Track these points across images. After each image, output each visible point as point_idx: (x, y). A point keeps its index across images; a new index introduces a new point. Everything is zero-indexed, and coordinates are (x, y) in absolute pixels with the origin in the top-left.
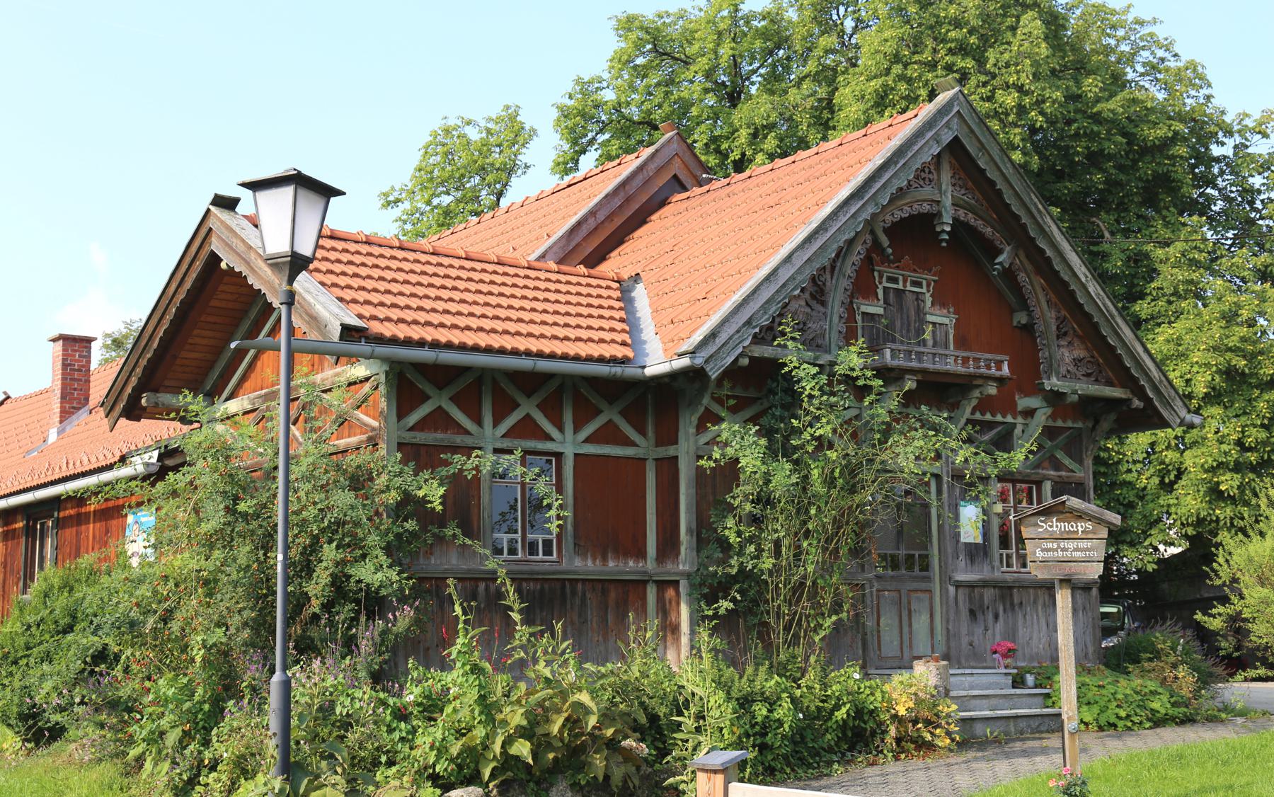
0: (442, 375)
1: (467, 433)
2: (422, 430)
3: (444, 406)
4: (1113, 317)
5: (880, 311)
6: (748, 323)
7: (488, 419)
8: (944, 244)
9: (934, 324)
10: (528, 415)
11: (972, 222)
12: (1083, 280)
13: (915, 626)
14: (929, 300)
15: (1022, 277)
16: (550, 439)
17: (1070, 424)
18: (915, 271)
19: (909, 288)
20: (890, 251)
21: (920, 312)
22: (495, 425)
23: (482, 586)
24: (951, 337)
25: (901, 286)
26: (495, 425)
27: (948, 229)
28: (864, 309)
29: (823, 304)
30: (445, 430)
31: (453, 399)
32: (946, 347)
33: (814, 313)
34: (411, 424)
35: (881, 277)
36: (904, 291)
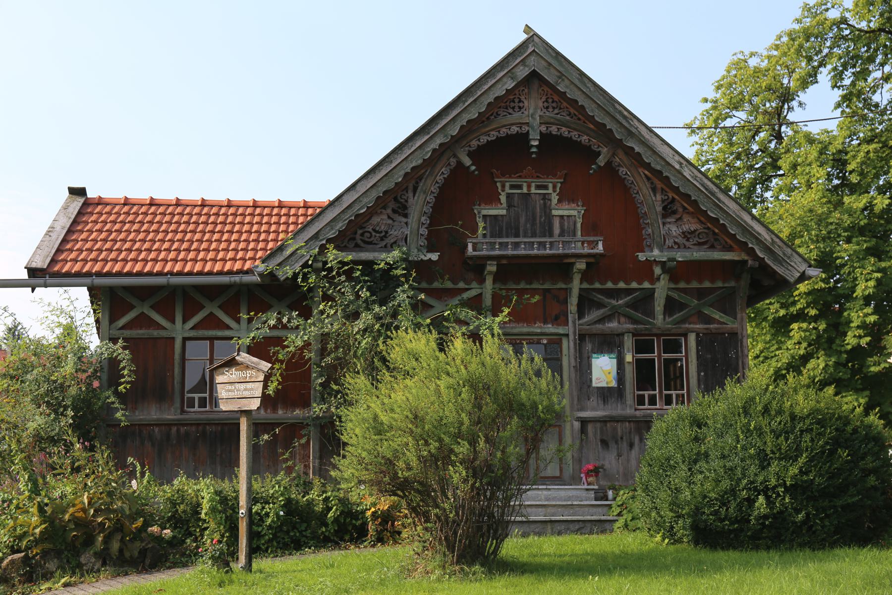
0: (143, 293)
1: (165, 328)
2: (131, 329)
3: (145, 312)
4: (713, 194)
5: (504, 212)
6: (316, 236)
8: (534, 156)
9: (562, 217)
11: (566, 134)
12: (677, 166)
14: (555, 198)
15: (623, 171)
16: (228, 327)
17: (719, 284)
18: (538, 177)
19: (533, 190)
20: (473, 168)
22: (184, 322)
23: (174, 429)
24: (579, 225)
25: (525, 190)
26: (184, 322)
27: (536, 143)
28: (485, 212)
29: (406, 216)
30: (148, 327)
31: (152, 307)
32: (574, 235)
33: (396, 223)
34: (120, 325)
35: (503, 186)
36: (529, 194)
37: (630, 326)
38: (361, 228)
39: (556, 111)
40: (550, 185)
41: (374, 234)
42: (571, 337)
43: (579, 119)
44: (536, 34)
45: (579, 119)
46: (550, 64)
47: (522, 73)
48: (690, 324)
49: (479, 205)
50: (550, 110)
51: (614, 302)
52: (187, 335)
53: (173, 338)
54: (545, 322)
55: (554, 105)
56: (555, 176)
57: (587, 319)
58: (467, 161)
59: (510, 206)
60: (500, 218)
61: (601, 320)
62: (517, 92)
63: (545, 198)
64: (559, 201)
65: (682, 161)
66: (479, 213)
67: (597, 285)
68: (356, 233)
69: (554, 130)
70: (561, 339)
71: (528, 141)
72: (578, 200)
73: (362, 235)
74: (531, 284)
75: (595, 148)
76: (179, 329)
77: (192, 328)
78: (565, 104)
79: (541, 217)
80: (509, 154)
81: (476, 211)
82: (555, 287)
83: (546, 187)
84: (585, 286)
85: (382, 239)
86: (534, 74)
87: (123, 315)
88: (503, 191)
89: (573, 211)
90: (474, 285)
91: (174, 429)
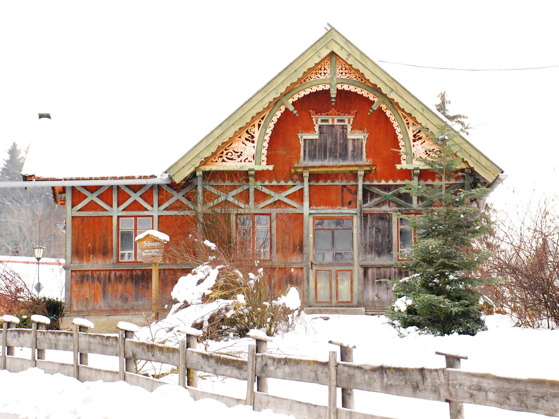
1: (106, 210)
7: (115, 204)
9: (354, 140)
10: (135, 201)
13: (340, 287)
14: (349, 128)
16: (146, 209)
19: (336, 123)
21: (344, 134)
23: (113, 273)
27: (335, 96)
29: (253, 142)
34: (78, 209)
35: (317, 121)
36: (333, 126)
37: (397, 209)
38: (226, 150)
39: (348, 75)
40: (347, 120)
41: (234, 153)
42: (359, 215)
43: (362, 80)
44: (333, 28)
45: (362, 80)
46: (342, 48)
47: (325, 53)
48: (435, 207)
49: (302, 133)
50: (344, 74)
51: (386, 193)
52: (120, 214)
53: (112, 216)
54: (343, 206)
55: (347, 71)
56: (349, 113)
57: (369, 203)
58: (291, 108)
59: (321, 133)
60: (314, 141)
61: (378, 205)
62: (323, 63)
63: (344, 128)
64: (352, 129)
65: (424, 107)
66: (302, 137)
67: (375, 183)
68: (222, 153)
69: (346, 87)
70: (353, 217)
71: (330, 94)
72: (364, 129)
73: (227, 154)
74: (333, 182)
75: (371, 98)
76: (115, 211)
77: (123, 210)
78: (353, 71)
79: (340, 139)
80: (318, 101)
81: (299, 137)
82: (348, 184)
83: (343, 121)
84: (367, 183)
85: (239, 157)
86: (333, 53)
87: (80, 202)
88: (317, 124)
89: (361, 136)
90: (298, 183)
91: (113, 273)
